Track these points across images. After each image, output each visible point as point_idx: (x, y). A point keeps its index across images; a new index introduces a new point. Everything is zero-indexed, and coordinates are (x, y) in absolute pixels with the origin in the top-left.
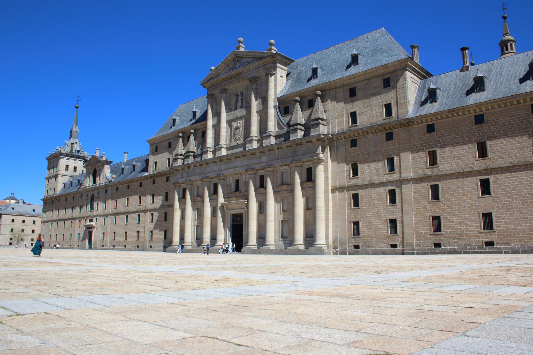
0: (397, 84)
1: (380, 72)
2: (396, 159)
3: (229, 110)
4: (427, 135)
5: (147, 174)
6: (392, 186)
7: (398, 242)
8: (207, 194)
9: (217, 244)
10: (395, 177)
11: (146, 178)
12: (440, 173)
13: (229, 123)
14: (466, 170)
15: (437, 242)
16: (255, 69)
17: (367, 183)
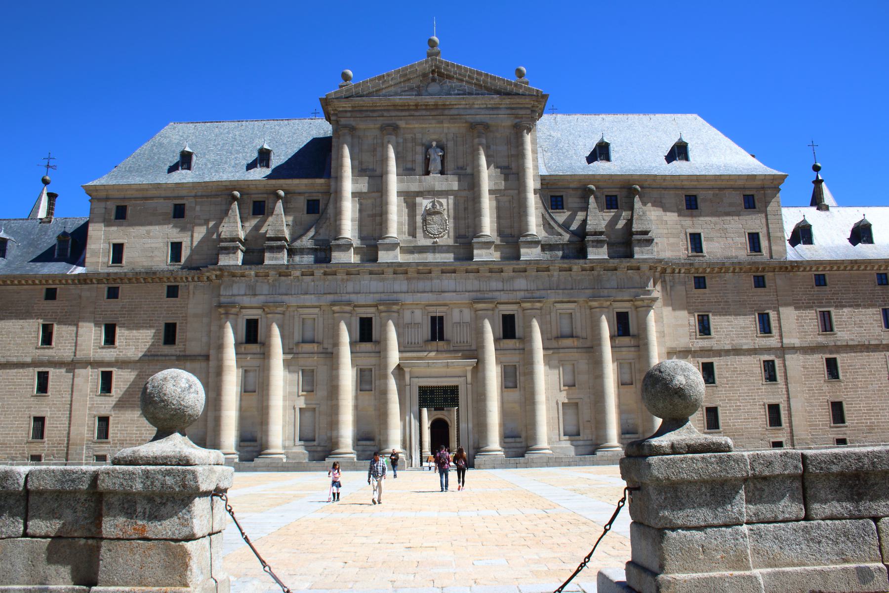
0: (766, 207)
1: (740, 183)
2: (773, 315)
3: (405, 170)
4: (816, 288)
5: (79, 270)
6: (769, 354)
7: (782, 437)
8: (345, 338)
9: (488, 448)
10: (772, 341)
11: (82, 280)
12: (839, 343)
13: (409, 198)
14: (872, 342)
15: (841, 437)
16: (487, 108)
17: (728, 347)
